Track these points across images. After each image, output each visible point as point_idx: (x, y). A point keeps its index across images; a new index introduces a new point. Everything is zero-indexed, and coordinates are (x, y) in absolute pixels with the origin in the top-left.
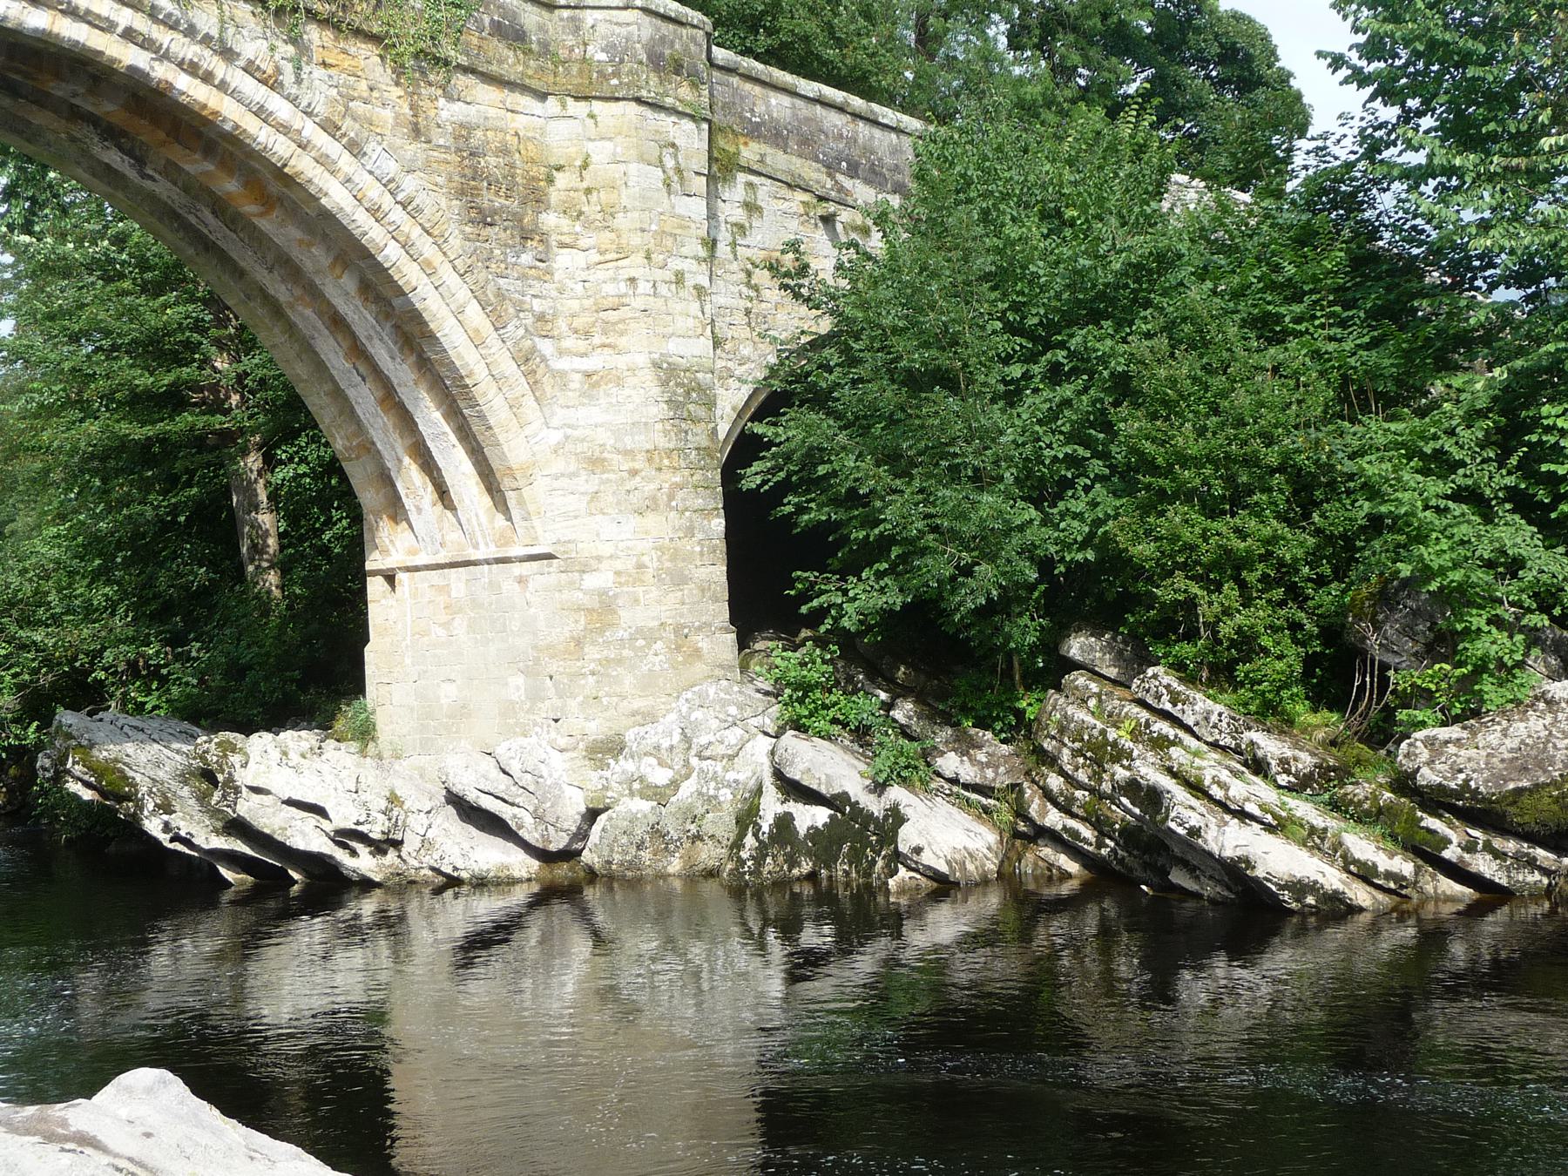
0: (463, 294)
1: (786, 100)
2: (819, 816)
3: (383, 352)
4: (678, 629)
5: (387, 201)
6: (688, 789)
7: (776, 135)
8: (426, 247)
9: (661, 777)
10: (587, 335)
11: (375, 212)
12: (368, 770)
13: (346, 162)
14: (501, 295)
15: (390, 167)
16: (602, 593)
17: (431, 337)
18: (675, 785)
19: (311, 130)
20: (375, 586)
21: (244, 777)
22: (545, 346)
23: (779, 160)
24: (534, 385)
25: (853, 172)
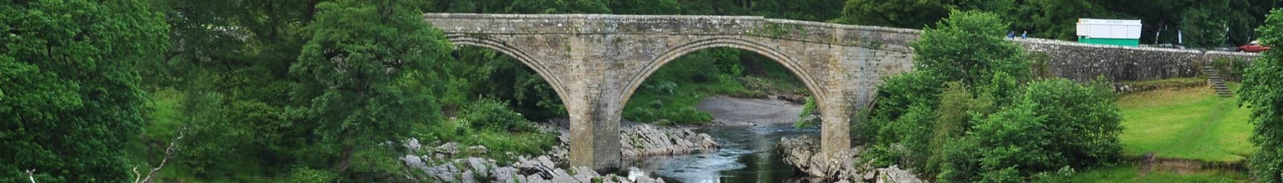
0: (810, 79)
5: (796, 65)
7: (891, 41)
8: (804, 72)
10: (833, 85)
13: (788, 60)
14: (817, 79)
15: (796, 60)
19: (781, 56)
22: (827, 87)
23: (892, 46)
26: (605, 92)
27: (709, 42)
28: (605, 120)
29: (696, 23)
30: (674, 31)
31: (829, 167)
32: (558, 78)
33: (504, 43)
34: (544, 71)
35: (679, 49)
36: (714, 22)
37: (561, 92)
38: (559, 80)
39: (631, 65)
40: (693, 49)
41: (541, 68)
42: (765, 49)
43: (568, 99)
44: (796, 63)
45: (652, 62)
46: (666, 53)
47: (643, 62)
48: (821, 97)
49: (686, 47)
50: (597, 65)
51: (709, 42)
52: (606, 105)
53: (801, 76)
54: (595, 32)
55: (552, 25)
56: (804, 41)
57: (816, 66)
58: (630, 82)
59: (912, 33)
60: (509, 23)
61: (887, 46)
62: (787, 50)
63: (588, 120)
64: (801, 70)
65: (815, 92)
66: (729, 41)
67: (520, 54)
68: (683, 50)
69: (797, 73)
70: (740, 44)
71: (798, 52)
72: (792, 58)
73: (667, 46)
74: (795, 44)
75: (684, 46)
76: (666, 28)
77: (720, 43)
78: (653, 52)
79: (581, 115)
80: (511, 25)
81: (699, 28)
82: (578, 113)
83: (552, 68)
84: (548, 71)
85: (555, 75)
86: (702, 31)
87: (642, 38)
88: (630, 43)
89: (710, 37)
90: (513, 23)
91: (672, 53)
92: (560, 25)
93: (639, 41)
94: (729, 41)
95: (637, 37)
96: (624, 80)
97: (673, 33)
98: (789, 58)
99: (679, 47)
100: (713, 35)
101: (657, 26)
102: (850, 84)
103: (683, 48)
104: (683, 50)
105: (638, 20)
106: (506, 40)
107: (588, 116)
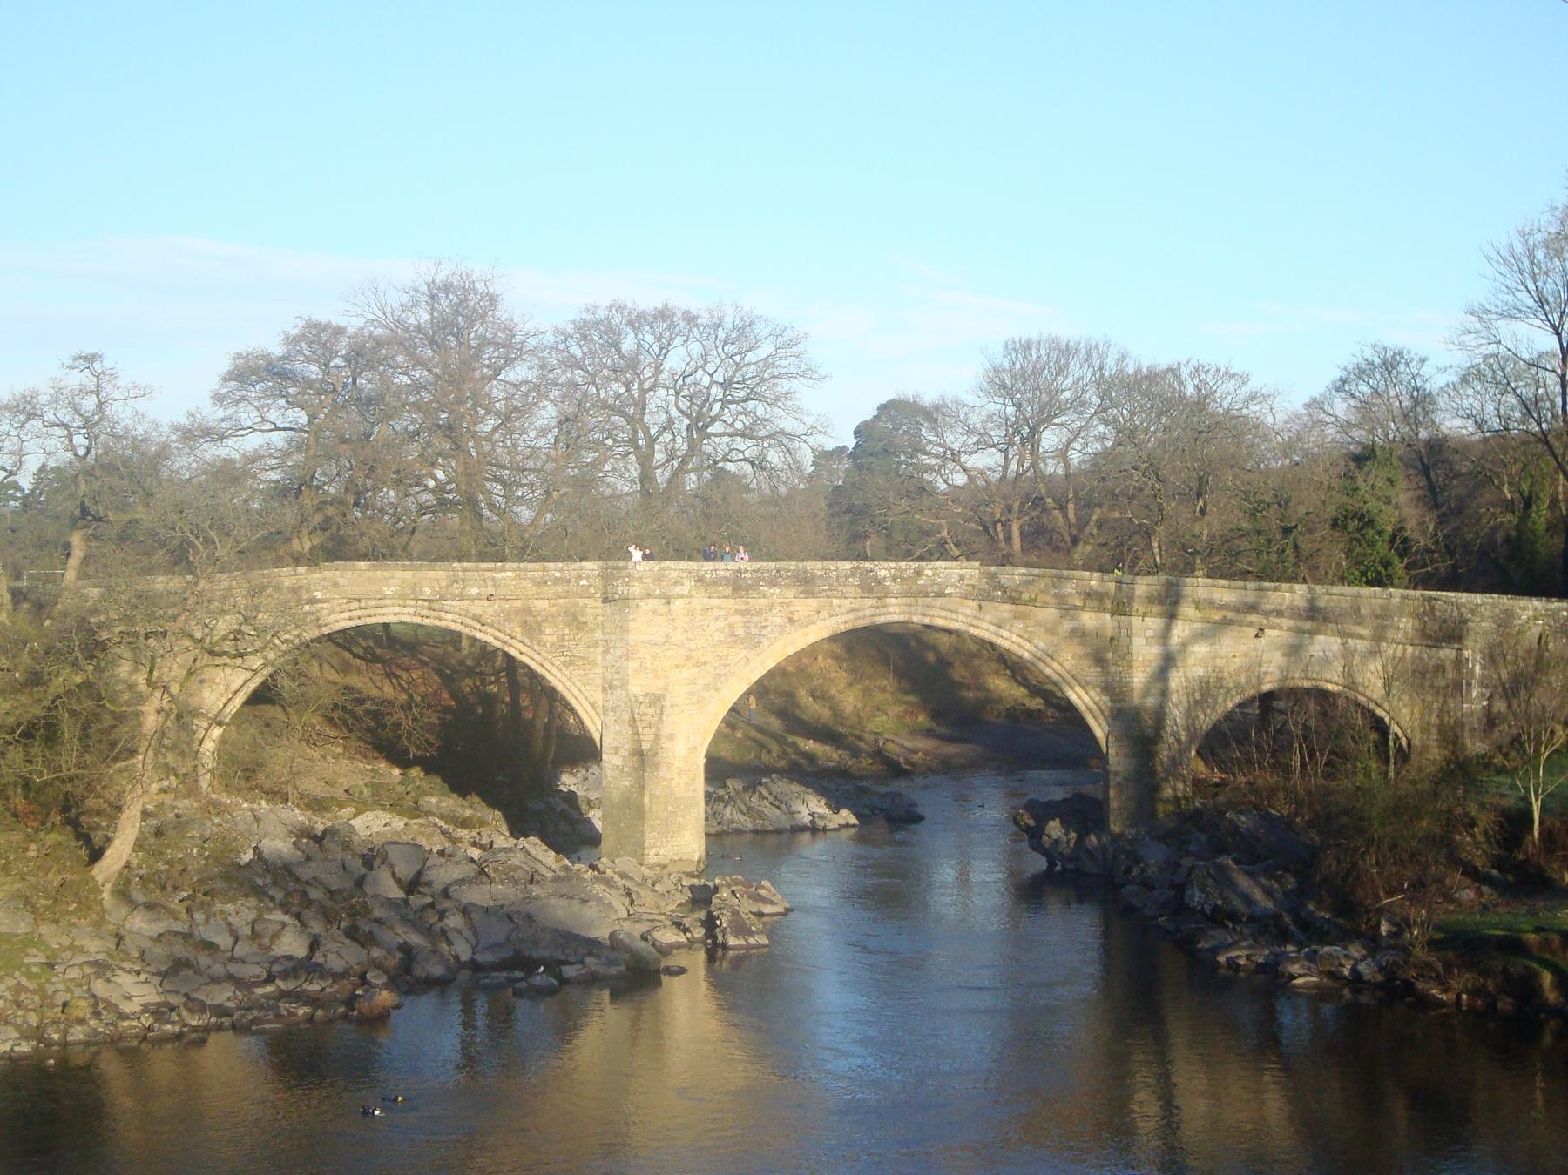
26: (670, 710)
28: (669, 766)
29: (847, 578)
31: (1115, 858)
32: (579, 684)
33: (477, 618)
36: (882, 573)
38: (582, 688)
39: (721, 657)
41: (549, 667)
52: (671, 737)
60: (484, 580)
62: (1026, 626)
67: (507, 638)
78: (764, 632)
80: (490, 583)
81: (855, 586)
82: (616, 753)
87: (743, 607)
90: (493, 579)
92: (583, 582)
105: (734, 571)
106: (479, 611)
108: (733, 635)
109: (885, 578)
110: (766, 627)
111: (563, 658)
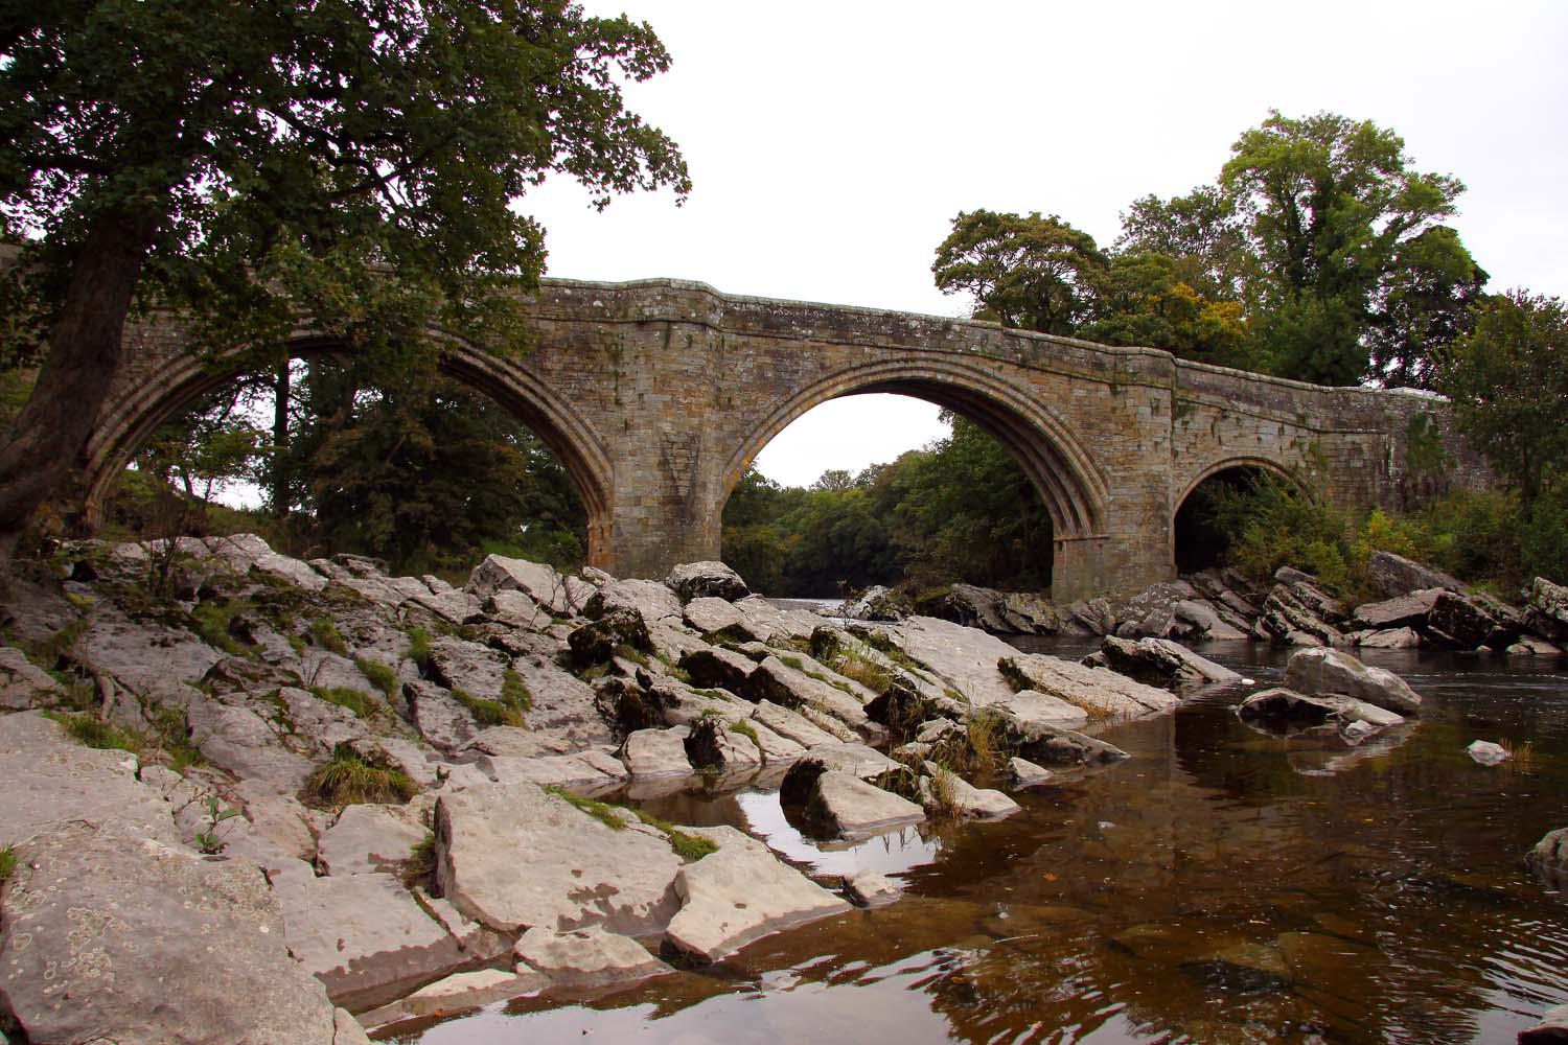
1: (1211, 376)
2: (1189, 628)
3: (1055, 469)
4: (1150, 564)
5: (1055, 424)
6: (1149, 617)
8: (1068, 438)
9: (1141, 613)
10: (1123, 464)
11: (1051, 427)
12: (1049, 610)
13: (1041, 412)
15: (1056, 412)
16: (1125, 551)
17: (1070, 465)
18: (1144, 617)
19: (1030, 403)
20: (1056, 547)
21: (1009, 606)
22: (1109, 468)
24: (1104, 481)
25: (1238, 398)
27: (902, 364)
28: (703, 520)
30: (836, 336)
32: (588, 422)
34: (558, 406)
35: (845, 377)
37: (595, 457)
38: (593, 428)
39: (748, 402)
40: (870, 379)
41: (551, 400)
42: (1003, 388)
43: (610, 473)
44: (1056, 419)
45: (791, 399)
46: (820, 382)
47: (774, 398)
48: (1097, 488)
49: (857, 373)
50: (689, 392)
51: (902, 364)
53: (1063, 446)
54: (684, 320)
55: (580, 301)
56: (1071, 377)
57: (1090, 426)
58: (746, 439)
59: (1235, 375)
61: (1198, 397)
63: (670, 516)
64: (1064, 433)
65: (1086, 477)
66: (938, 366)
67: (503, 364)
68: (850, 380)
69: (1056, 438)
70: (957, 375)
71: (1060, 397)
72: (1050, 408)
73: (823, 367)
74: (1054, 380)
75: (854, 369)
76: (823, 328)
77: (922, 369)
78: (795, 377)
79: (649, 508)
81: (886, 335)
83: (577, 398)
84: (567, 406)
85: (583, 416)
86: (891, 340)
88: (748, 355)
89: (903, 355)
91: (831, 382)
92: (598, 303)
93: (767, 352)
94: (938, 366)
95: (764, 344)
96: (734, 434)
97: (836, 340)
98: (1044, 408)
99: (844, 372)
100: (910, 350)
101: (805, 324)
102: (1157, 460)
103: (851, 374)
104: (850, 380)
107: (667, 509)
108: (762, 376)
109: (916, 328)
110: (797, 372)
111: (570, 392)
